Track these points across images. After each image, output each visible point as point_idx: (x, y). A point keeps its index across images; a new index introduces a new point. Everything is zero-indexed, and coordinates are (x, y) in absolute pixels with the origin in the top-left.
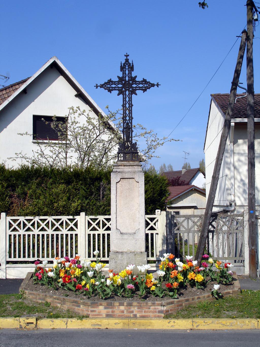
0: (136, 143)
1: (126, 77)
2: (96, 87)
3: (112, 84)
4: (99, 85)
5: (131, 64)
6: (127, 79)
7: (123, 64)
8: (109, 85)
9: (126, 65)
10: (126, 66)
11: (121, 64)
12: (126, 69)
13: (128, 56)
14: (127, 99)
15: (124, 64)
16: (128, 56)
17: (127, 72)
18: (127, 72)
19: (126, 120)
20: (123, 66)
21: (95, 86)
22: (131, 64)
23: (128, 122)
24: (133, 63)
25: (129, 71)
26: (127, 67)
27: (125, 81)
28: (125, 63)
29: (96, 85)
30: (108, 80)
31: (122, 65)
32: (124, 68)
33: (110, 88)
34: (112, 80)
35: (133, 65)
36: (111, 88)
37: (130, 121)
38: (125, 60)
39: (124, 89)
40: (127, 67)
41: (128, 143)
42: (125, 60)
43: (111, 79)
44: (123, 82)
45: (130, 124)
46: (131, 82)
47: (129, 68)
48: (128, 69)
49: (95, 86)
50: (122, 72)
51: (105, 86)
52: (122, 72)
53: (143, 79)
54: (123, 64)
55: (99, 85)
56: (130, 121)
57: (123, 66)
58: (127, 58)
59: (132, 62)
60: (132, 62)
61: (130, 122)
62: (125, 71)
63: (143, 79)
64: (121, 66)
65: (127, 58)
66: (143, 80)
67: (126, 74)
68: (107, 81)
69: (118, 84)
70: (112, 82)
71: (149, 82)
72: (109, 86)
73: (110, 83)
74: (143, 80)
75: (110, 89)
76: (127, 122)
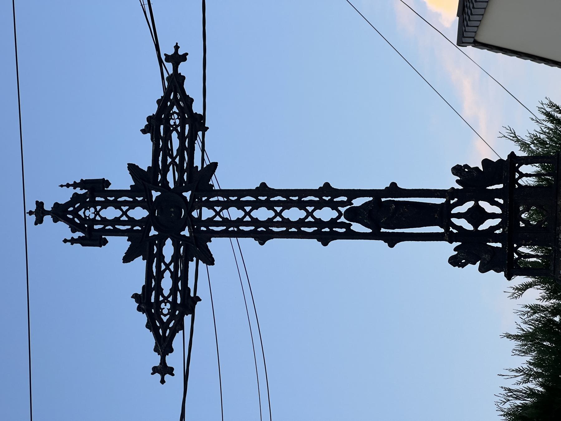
0: (457, 170)
1: (132, 221)
2: (167, 377)
3: (159, 291)
4: (156, 360)
5: (79, 191)
6: (139, 213)
7: (73, 231)
8: (163, 305)
9: (79, 217)
10: (84, 220)
11: (73, 241)
12: (98, 218)
13: (40, 205)
14: (234, 213)
15: (74, 228)
16: (40, 205)
17: (111, 213)
18: (111, 213)
19: (333, 223)
20: (82, 235)
21: (163, 382)
22: (79, 191)
23: (343, 210)
24: (75, 185)
25: (105, 205)
26: (90, 213)
27: (145, 223)
28: (70, 223)
29: (158, 376)
30: (139, 309)
31: (78, 235)
32: (91, 227)
33: (174, 304)
34: (140, 292)
35: (83, 184)
36: (175, 299)
37: (343, 204)
38: (55, 221)
39: (186, 233)
40: (90, 213)
41: (459, 216)
42: (55, 221)
43: (135, 296)
44: (153, 232)
45: (358, 202)
46: (155, 194)
47: (94, 204)
48: (98, 208)
49: (163, 382)
50: (107, 237)
51: (165, 326)
52: (107, 237)
53: (144, 131)
54: (73, 231)
55: (156, 360)
56: (343, 204)
57: (82, 235)
58: (48, 213)
59: (68, 185)
60: (68, 185)
61: (345, 199)
62: (104, 221)
63: (144, 131)
64: (82, 241)
65: (48, 213)
66: (149, 135)
67: (117, 221)
68: (143, 318)
69: (161, 258)
70: (147, 289)
71: (162, 103)
72: (166, 308)
73: (153, 300)
74: (149, 135)
75: (179, 301)
76: (343, 219)
